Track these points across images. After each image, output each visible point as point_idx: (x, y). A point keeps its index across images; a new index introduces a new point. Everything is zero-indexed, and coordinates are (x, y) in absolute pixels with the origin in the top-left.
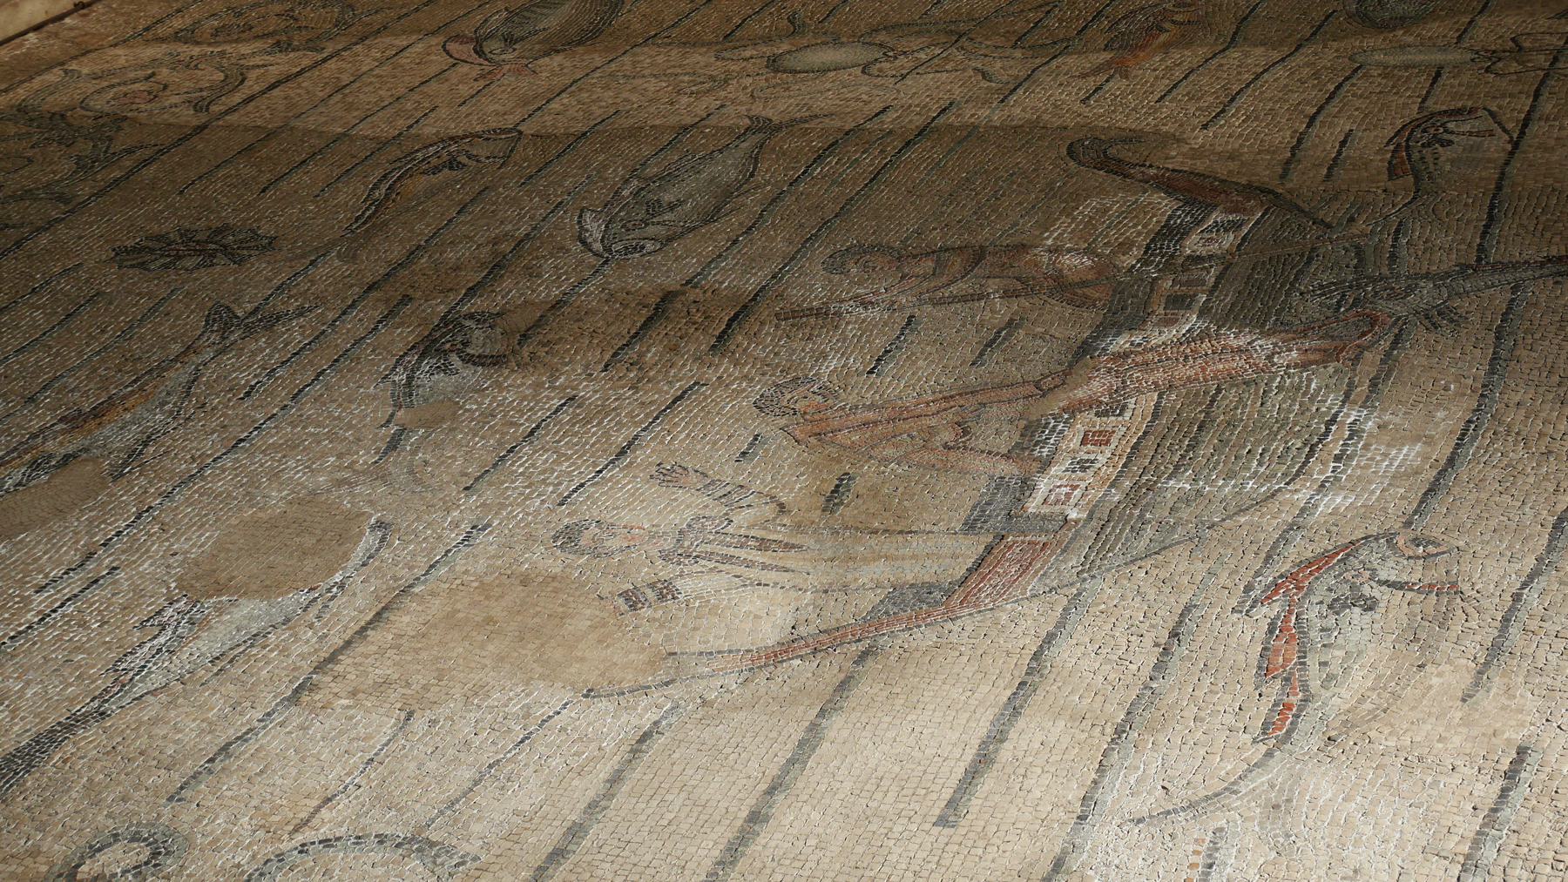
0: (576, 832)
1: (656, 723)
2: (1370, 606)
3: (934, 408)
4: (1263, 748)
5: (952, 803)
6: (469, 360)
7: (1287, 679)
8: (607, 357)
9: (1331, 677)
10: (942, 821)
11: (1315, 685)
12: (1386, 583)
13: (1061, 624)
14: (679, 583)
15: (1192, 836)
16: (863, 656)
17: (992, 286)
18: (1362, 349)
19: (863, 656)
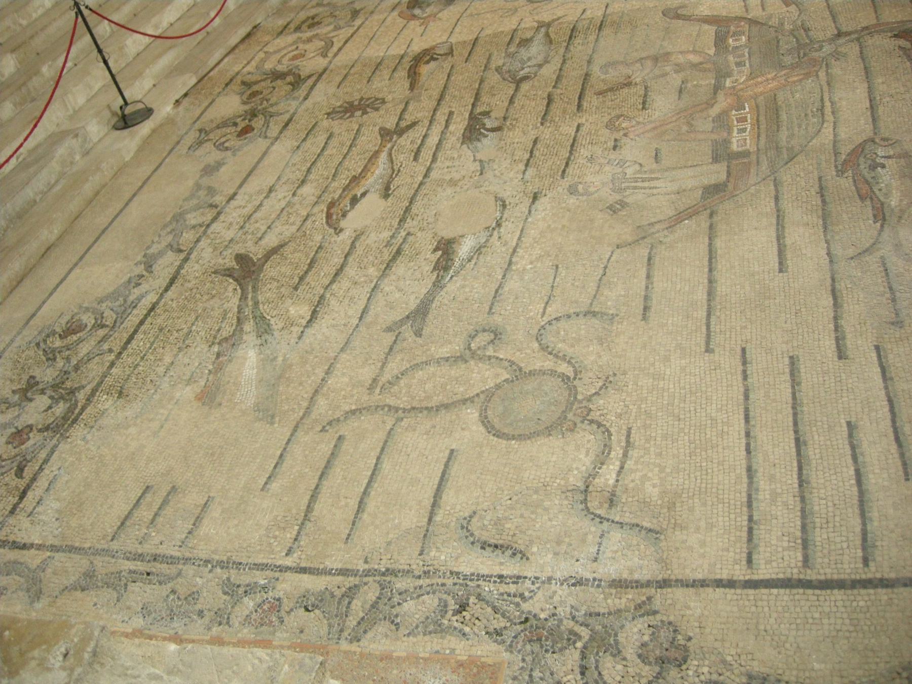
0: (646, 298)
1: (650, 253)
2: (883, 166)
3: (674, 119)
4: (878, 224)
5: (781, 263)
6: (488, 130)
7: (871, 199)
8: (540, 120)
9: (886, 194)
10: (781, 271)
11: (882, 198)
12: (883, 157)
13: (777, 191)
14: (625, 200)
15: (872, 260)
16: (711, 216)
17: (668, 69)
18: (817, 72)
19: (711, 216)
